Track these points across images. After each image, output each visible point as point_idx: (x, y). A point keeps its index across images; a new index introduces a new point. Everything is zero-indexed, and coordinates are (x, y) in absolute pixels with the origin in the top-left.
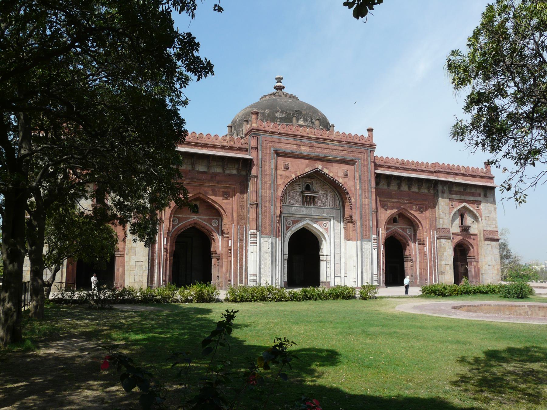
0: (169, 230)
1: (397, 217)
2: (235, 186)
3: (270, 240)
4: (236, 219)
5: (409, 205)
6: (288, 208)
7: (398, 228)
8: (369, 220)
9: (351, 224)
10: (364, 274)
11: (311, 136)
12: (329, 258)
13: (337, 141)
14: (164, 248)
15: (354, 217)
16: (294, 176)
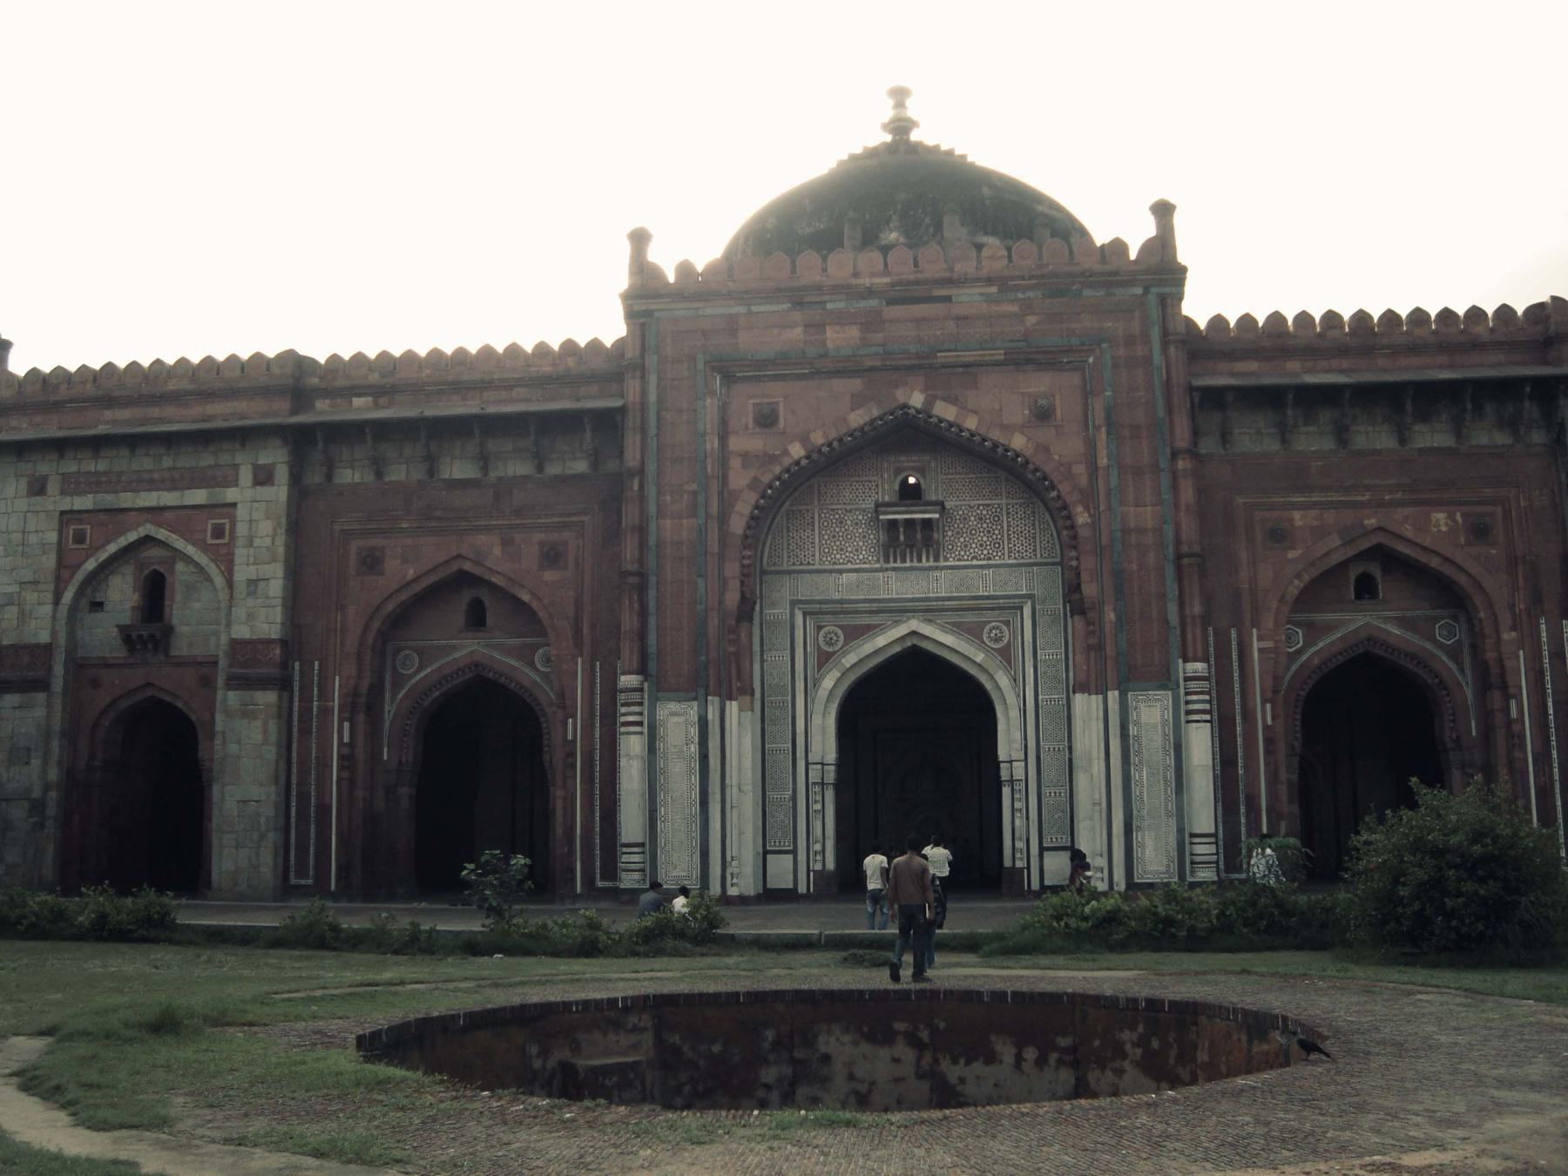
0: (355, 693)
1: (1377, 573)
2: (584, 518)
3: (693, 710)
4: (587, 639)
5: (1408, 511)
6: (818, 578)
7: (1386, 619)
8: (1162, 596)
9: (1079, 622)
10: (1137, 837)
11: (867, 281)
12: (1019, 773)
13: (989, 281)
14: (341, 757)
15: (1089, 590)
16: (797, 451)
